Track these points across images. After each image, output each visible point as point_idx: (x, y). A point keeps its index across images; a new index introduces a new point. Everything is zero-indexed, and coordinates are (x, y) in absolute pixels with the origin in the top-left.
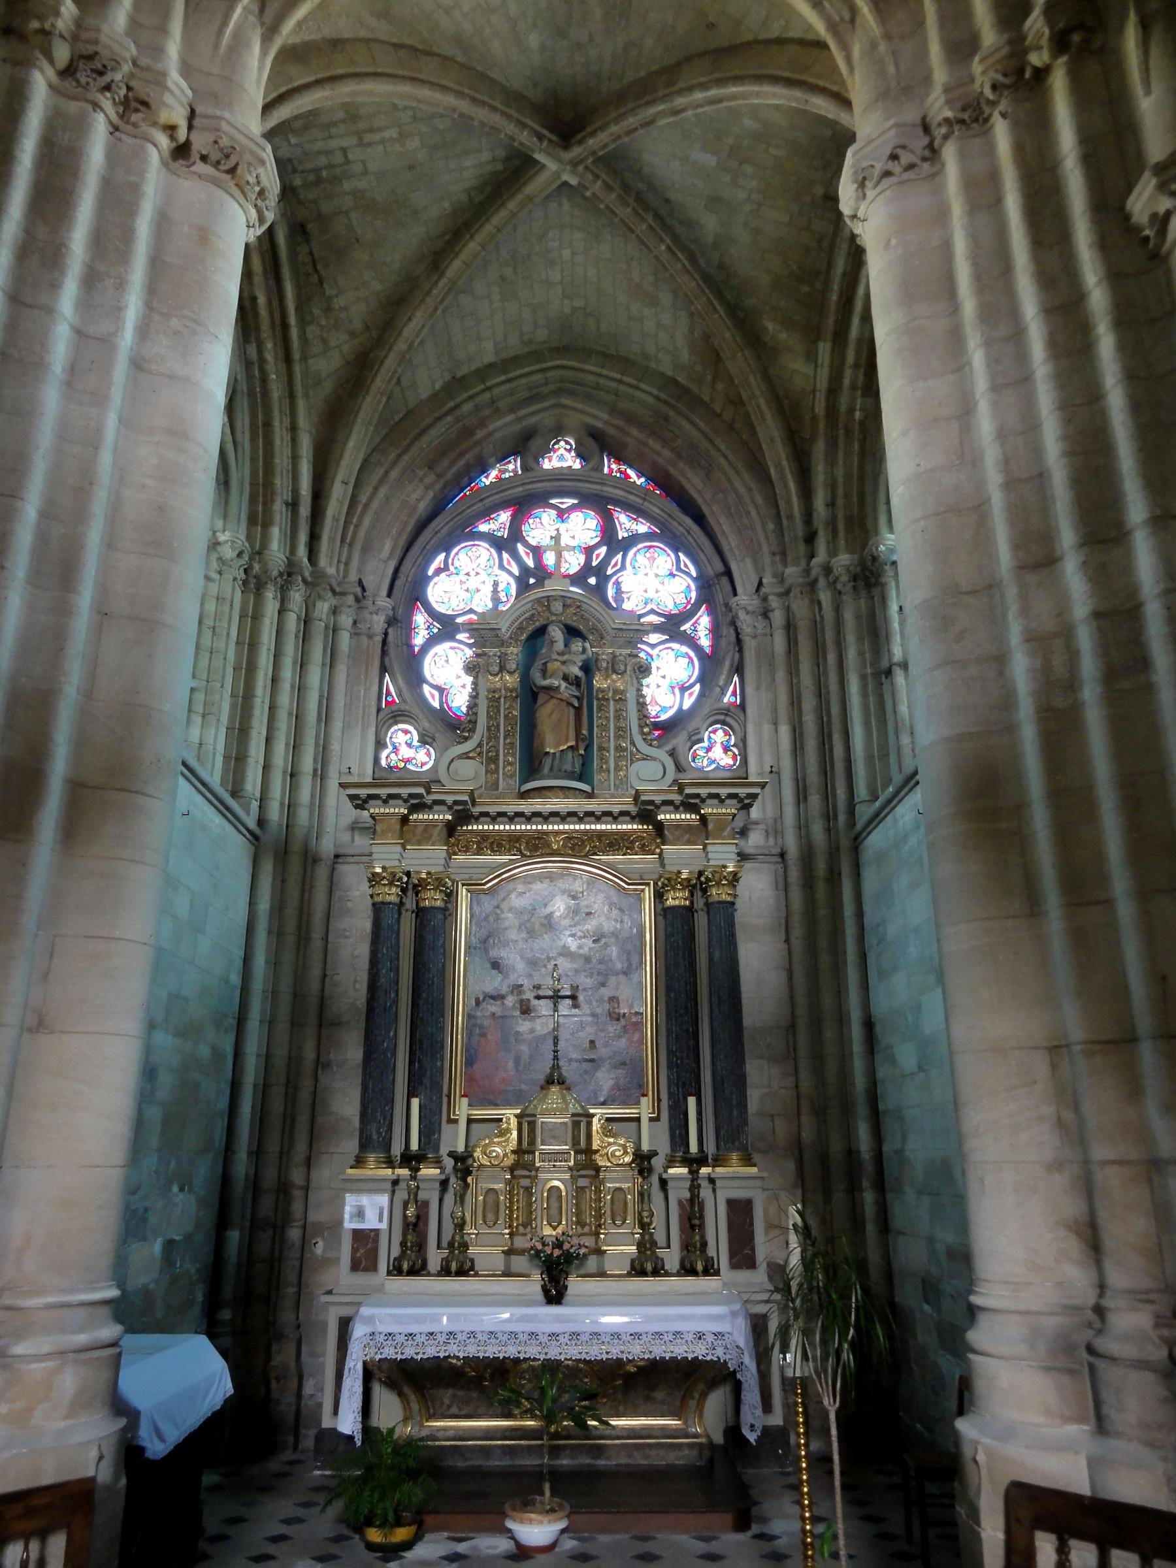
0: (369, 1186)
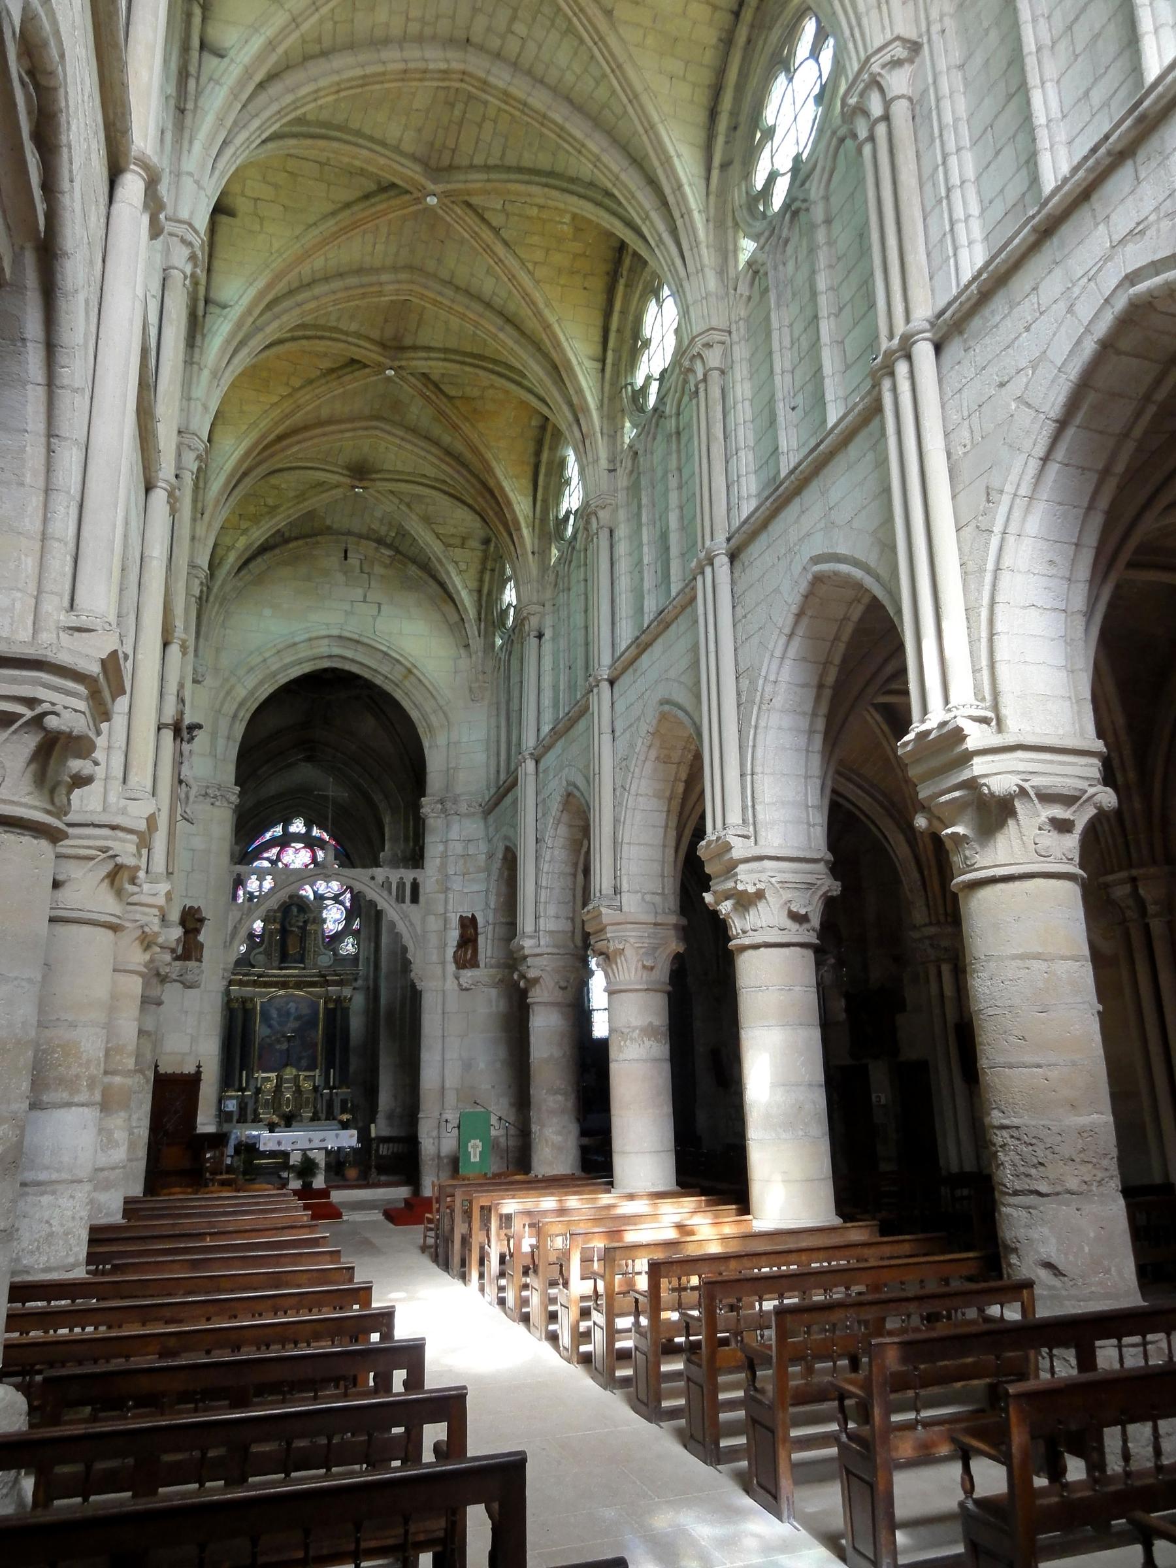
0: (230, 1098)
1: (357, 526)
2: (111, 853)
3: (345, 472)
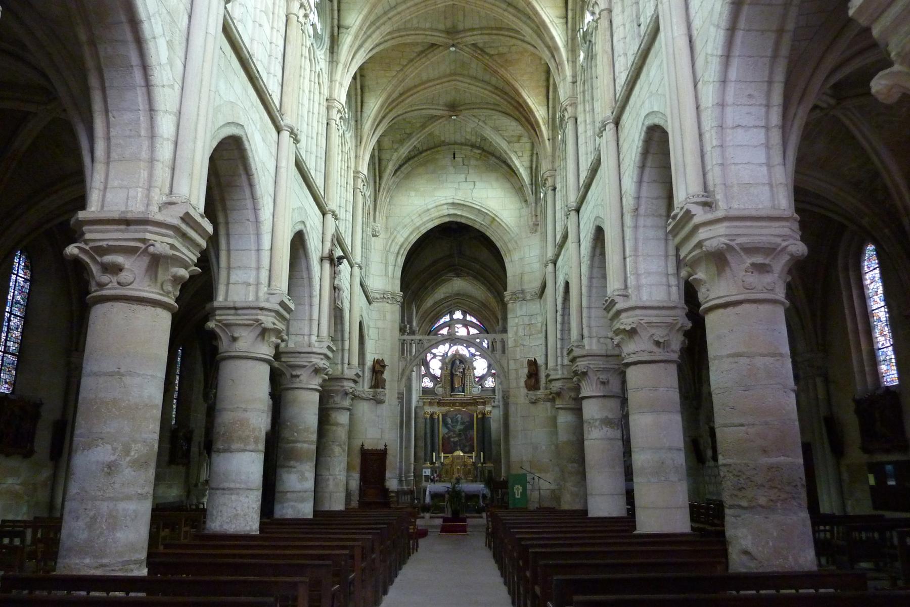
0: (427, 468)
1: (459, 138)
2: (260, 322)
3: (444, 108)
